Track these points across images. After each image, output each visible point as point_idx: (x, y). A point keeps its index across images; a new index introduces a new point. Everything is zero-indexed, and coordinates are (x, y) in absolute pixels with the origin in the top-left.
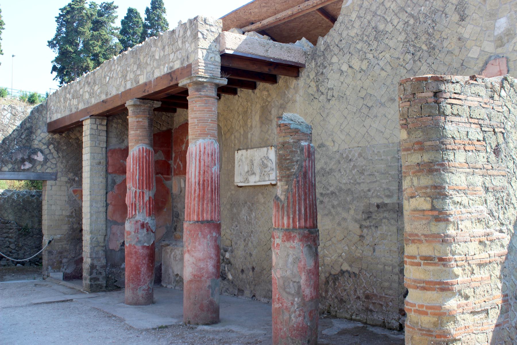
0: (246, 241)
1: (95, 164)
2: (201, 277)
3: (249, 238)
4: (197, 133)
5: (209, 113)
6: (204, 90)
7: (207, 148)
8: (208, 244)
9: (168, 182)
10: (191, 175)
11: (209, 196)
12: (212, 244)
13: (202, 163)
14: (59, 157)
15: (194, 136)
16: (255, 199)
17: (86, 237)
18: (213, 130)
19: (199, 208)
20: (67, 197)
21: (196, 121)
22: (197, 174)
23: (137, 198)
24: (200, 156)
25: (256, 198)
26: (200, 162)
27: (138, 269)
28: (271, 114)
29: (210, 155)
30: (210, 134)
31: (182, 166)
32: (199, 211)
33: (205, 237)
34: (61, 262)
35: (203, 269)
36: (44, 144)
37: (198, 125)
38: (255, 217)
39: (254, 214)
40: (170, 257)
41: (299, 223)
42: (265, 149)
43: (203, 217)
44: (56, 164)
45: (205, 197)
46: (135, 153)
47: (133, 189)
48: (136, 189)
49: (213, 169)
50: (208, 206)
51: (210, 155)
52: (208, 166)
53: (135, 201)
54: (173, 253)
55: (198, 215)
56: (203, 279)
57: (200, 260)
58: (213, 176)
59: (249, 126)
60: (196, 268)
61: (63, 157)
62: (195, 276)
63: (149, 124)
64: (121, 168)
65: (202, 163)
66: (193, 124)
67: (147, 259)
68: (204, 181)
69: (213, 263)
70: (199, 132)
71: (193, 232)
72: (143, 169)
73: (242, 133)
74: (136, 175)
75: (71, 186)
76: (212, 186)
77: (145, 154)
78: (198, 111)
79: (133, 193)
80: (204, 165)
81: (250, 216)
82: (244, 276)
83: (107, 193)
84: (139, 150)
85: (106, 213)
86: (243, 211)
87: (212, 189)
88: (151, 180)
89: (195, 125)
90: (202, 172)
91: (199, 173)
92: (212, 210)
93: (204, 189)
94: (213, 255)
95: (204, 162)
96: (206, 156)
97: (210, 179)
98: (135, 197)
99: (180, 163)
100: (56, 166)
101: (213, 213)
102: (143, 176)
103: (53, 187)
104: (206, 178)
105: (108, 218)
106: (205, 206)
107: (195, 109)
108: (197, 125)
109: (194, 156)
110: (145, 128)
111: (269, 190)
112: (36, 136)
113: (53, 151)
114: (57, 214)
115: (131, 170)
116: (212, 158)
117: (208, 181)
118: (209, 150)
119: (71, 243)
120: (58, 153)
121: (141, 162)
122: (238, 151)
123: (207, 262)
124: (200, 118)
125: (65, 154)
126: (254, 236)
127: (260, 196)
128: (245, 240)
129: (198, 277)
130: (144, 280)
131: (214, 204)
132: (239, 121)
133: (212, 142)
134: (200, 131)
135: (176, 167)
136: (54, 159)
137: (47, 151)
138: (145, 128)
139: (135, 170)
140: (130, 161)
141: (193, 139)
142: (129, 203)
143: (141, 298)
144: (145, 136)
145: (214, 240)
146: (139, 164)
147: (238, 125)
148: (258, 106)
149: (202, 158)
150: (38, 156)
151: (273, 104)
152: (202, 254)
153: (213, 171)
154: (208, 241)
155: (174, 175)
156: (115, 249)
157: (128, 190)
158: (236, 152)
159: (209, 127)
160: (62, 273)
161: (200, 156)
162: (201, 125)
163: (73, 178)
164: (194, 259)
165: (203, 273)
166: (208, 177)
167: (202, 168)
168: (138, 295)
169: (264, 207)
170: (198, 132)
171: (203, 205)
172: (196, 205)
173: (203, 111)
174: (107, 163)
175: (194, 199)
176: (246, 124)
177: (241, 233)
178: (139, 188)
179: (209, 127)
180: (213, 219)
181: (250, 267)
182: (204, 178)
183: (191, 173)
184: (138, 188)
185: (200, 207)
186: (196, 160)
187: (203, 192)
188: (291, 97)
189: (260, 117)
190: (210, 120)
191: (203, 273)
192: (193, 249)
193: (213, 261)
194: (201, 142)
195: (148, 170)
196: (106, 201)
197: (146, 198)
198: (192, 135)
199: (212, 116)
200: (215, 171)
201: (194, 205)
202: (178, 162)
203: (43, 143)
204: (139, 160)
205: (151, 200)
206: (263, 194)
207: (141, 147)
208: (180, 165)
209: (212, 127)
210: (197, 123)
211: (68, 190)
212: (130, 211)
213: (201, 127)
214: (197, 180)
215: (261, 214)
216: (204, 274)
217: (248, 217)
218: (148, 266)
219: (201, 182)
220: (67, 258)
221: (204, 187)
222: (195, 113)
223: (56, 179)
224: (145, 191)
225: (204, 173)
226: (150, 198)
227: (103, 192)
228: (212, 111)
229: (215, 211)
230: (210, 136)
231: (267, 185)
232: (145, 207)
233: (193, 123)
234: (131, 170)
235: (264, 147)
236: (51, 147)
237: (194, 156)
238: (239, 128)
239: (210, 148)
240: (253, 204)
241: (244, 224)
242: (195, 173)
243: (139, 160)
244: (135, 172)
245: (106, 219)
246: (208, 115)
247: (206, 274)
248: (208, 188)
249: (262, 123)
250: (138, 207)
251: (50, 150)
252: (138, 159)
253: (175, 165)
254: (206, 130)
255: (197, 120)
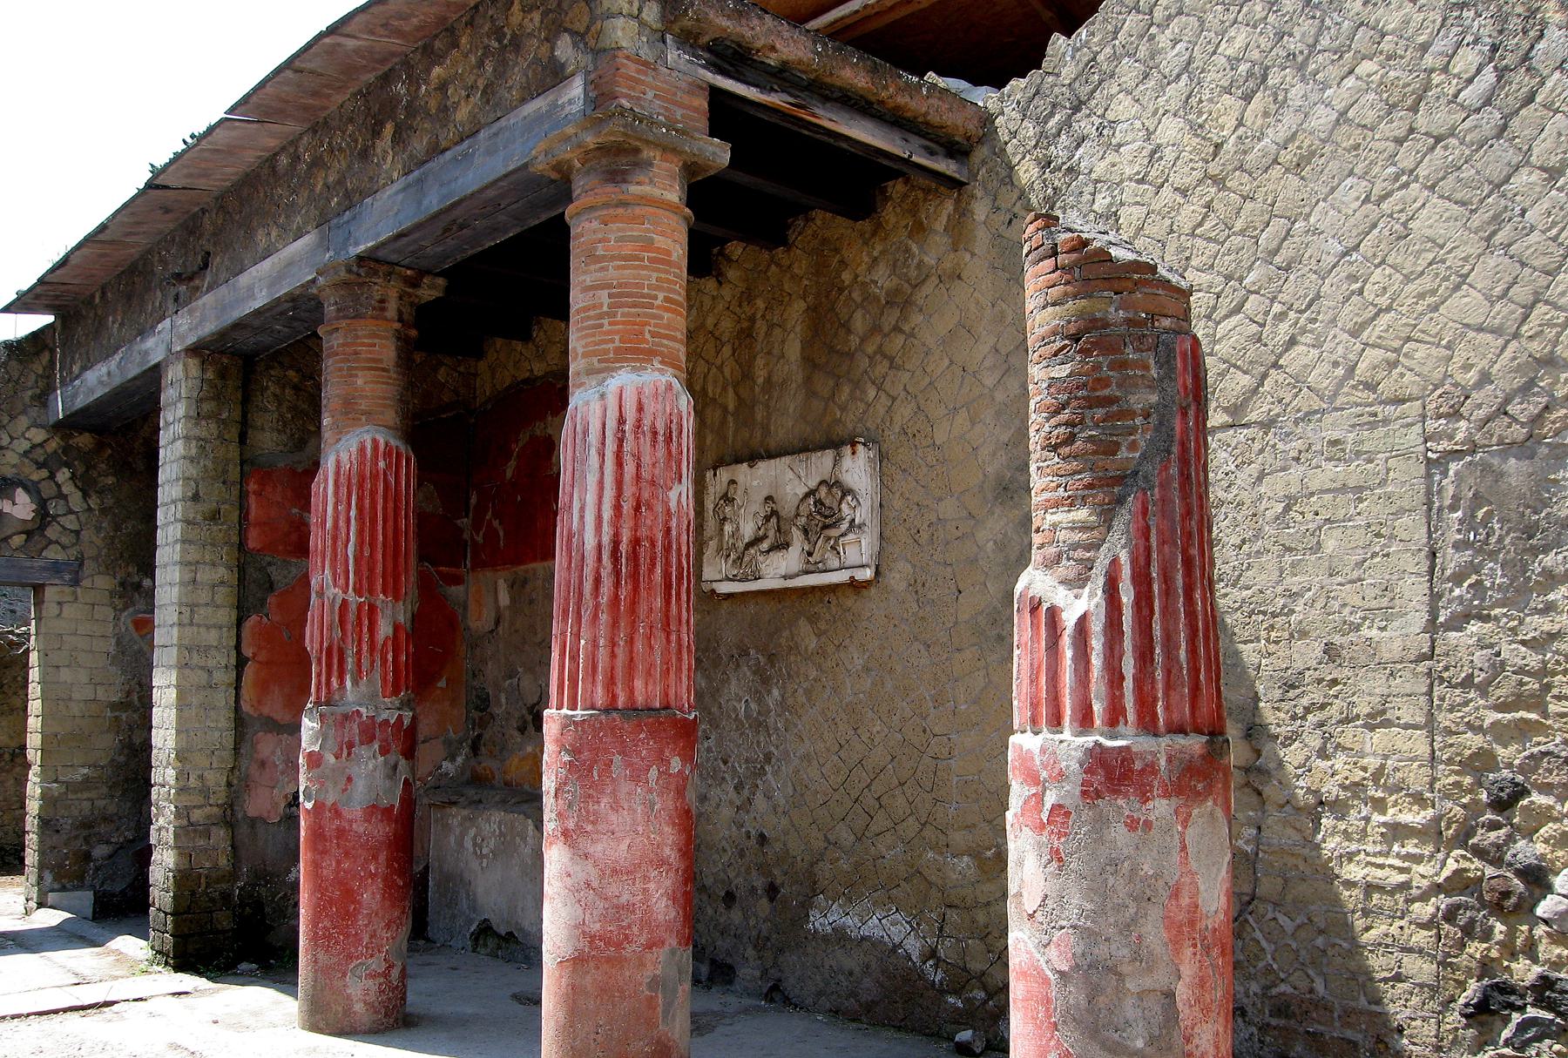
0: (746, 792)
1: (199, 518)
2: (619, 945)
3: (759, 782)
4: (611, 346)
5: (658, 270)
6: (641, 178)
7: (650, 407)
8: (652, 804)
9: (455, 591)
10: (582, 517)
11: (658, 603)
12: (664, 804)
13: (630, 469)
14: (90, 509)
15: (595, 360)
16: (783, 641)
17: (164, 774)
18: (673, 339)
19: (613, 655)
20: (113, 641)
21: (606, 301)
22: (607, 514)
23: (349, 627)
24: (621, 441)
25: (786, 633)
26: (619, 463)
27: (349, 895)
28: (849, 331)
29: (661, 438)
30: (661, 354)
31: (501, 534)
32: (613, 668)
33: (637, 777)
34: (87, 857)
35: (629, 908)
36: (40, 466)
37: (615, 315)
38: (782, 704)
39: (776, 692)
40: (460, 844)
41: (1167, 708)
42: (828, 457)
43: (632, 691)
44: (77, 533)
45: (643, 608)
46: (344, 457)
47: (334, 592)
48: (345, 592)
49: (673, 495)
50: (651, 647)
51: (661, 438)
52: (653, 483)
53: (343, 639)
54: (472, 832)
55: (611, 682)
56: (629, 950)
57: (615, 871)
58: (674, 523)
59: (760, 381)
60: (601, 904)
61: (104, 511)
62: (593, 937)
63: (399, 357)
64: (294, 537)
65: (630, 469)
66: (591, 313)
67: (382, 857)
68: (636, 542)
69: (668, 883)
70: (617, 344)
71: (586, 755)
72: (373, 521)
73: (731, 407)
74: (348, 540)
75: (126, 608)
76: (667, 564)
77: (382, 464)
78: (613, 258)
79: (332, 611)
80: (638, 477)
81: (760, 701)
82: (736, 916)
83: (239, 623)
84: (362, 450)
85: (238, 688)
86: (734, 682)
87: (667, 575)
88: (402, 560)
89: (601, 316)
90: (627, 507)
91: (617, 508)
92: (667, 662)
93: (634, 576)
94: (670, 853)
95: (638, 466)
96: (646, 442)
97: (660, 536)
98: (342, 622)
99: (496, 523)
100: (78, 539)
101: (672, 675)
102: (372, 545)
103: (66, 608)
104: (643, 532)
105: (246, 707)
106: (639, 646)
107: (600, 252)
108: (607, 314)
109: (594, 438)
110: (384, 370)
111: (839, 605)
112: (12, 438)
113: (68, 489)
114: (76, 696)
115: (329, 524)
116: (670, 452)
117: (653, 545)
118: (656, 414)
119: (123, 794)
120: (86, 495)
121: (367, 493)
122: (715, 469)
123: (646, 879)
124: (620, 285)
125: (109, 501)
126: (776, 773)
127: (804, 626)
128: (738, 788)
129: (608, 943)
130: (371, 937)
131: (673, 637)
132: (720, 368)
133: (669, 387)
134: (621, 341)
135: (480, 539)
136: (72, 517)
137: (47, 490)
138: (384, 370)
139: (342, 524)
140: (325, 489)
141: (591, 372)
142: (316, 646)
143: (359, 1007)
144: (385, 398)
145: (673, 787)
146: (360, 499)
147: (715, 382)
148: (799, 306)
149: (627, 447)
150: (14, 504)
151: (856, 295)
152: (624, 847)
153: (673, 505)
154: (650, 791)
155: (473, 568)
156: (265, 815)
157: (313, 596)
158: (709, 474)
159: (656, 325)
160: (90, 894)
161: (621, 441)
162: (623, 315)
163: (136, 579)
164: (590, 868)
165: (629, 927)
166: (651, 528)
167: (629, 490)
168: (349, 997)
169: (819, 668)
170: (612, 341)
171: (631, 641)
172: (602, 642)
173: (637, 258)
174: (244, 516)
175: (595, 617)
176: (747, 375)
177: (725, 762)
178: (358, 592)
179: (656, 325)
180: (673, 704)
181: (759, 882)
182: (636, 528)
183: (582, 509)
184: (354, 590)
185: (621, 652)
186: (602, 455)
187: (630, 587)
188: (933, 262)
189: (807, 345)
190: (661, 296)
191: (629, 927)
192: (589, 828)
193: (671, 874)
194: (625, 380)
195: (391, 523)
196: (238, 647)
197: (384, 629)
198: (585, 355)
199: (669, 281)
200: (679, 502)
201: (595, 644)
202: (490, 521)
203: (37, 463)
204: (360, 482)
205: (403, 637)
206: (813, 620)
207: (368, 438)
208: (496, 531)
209: (668, 327)
210: (610, 306)
211: (117, 618)
212: (319, 675)
213: (624, 323)
214: (606, 539)
215: (808, 692)
216: (635, 930)
217: (753, 706)
218: (389, 885)
219: (623, 548)
220: (108, 842)
221: (636, 566)
222: (602, 269)
223: (76, 582)
224: (378, 603)
225: (637, 509)
226: (396, 628)
227: (226, 616)
228: (669, 263)
229: (679, 669)
230: (661, 363)
231: (833, 588)
232: (378, 662)
233: (594, 307)
234: (329, 524)
235: (823, 448)
236: (63, 475)
237: (594, 438)
238: (718, 391)
239: (660, 407)
240: (771, 658)
241: (737, 729)
242: (599, 510)
243: (361, 486)
244: (343, 531)
245: (237, 708)
246: (655, 275)
247: (641, 930)
248: (651, 570)
249: (809, 361)
250: (350, 662)
251: (59, 486)
252: (354, 481)
253: (478, 535)
254: (648, 336)
255: (610, 296)
